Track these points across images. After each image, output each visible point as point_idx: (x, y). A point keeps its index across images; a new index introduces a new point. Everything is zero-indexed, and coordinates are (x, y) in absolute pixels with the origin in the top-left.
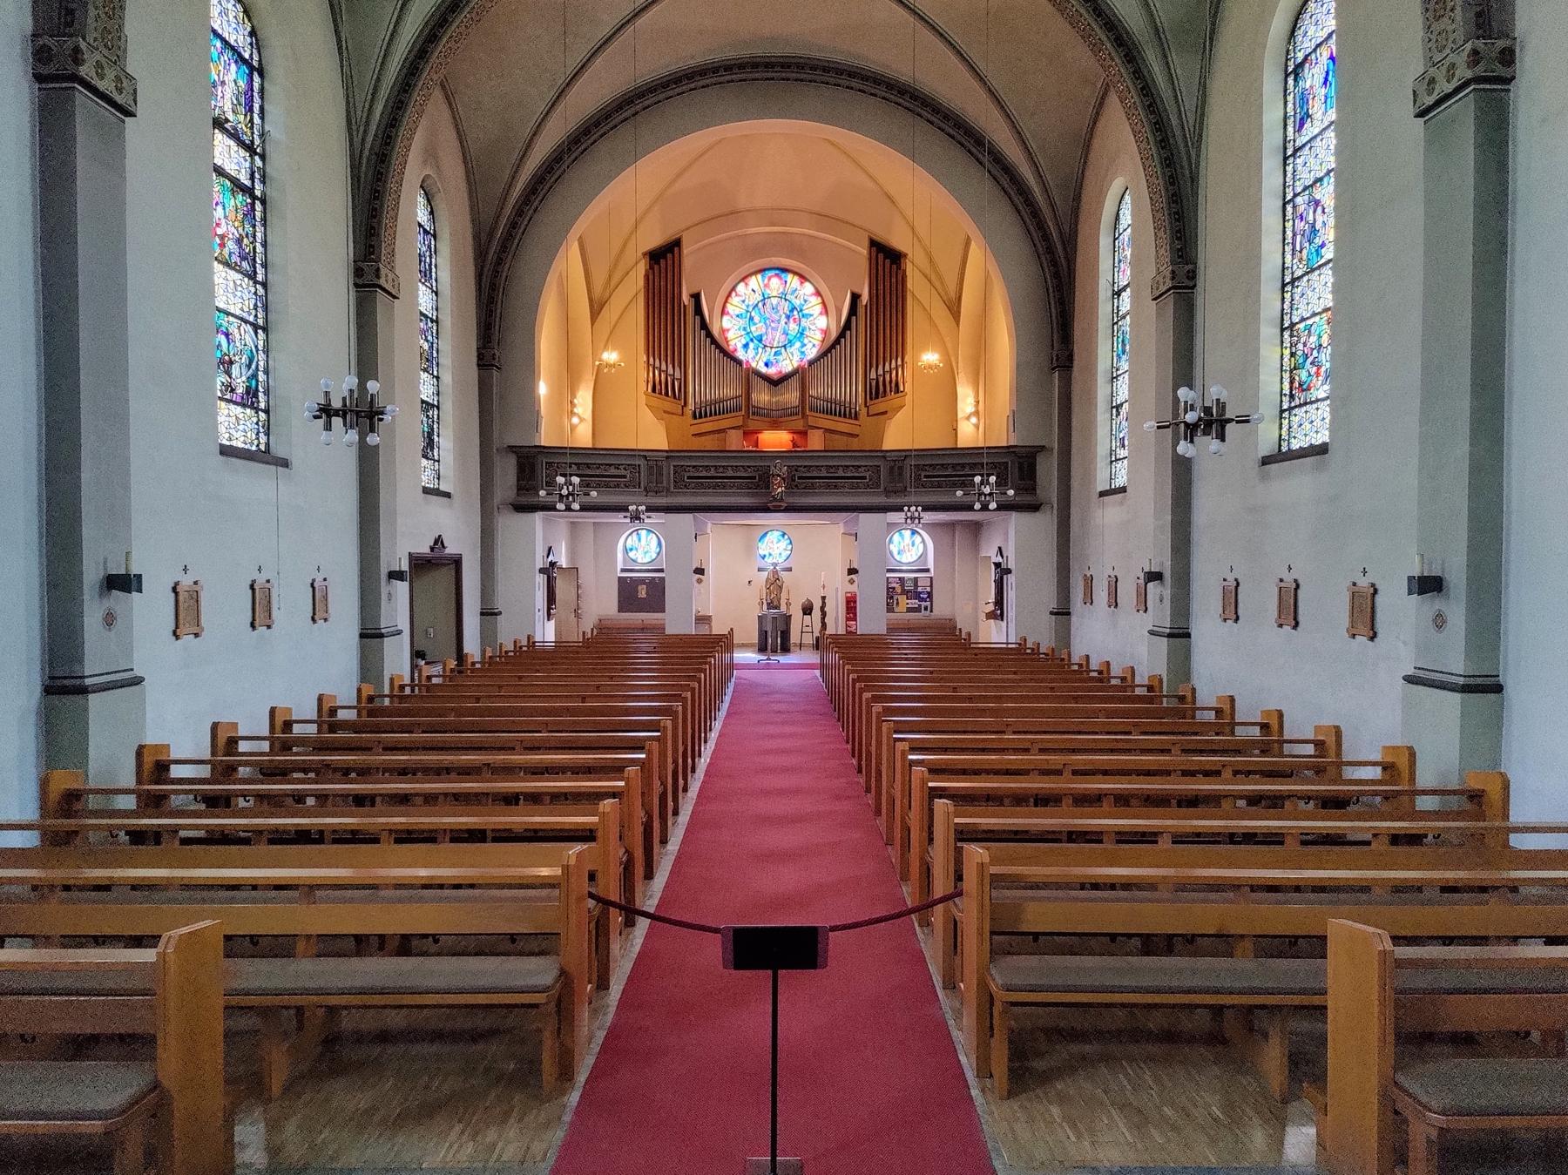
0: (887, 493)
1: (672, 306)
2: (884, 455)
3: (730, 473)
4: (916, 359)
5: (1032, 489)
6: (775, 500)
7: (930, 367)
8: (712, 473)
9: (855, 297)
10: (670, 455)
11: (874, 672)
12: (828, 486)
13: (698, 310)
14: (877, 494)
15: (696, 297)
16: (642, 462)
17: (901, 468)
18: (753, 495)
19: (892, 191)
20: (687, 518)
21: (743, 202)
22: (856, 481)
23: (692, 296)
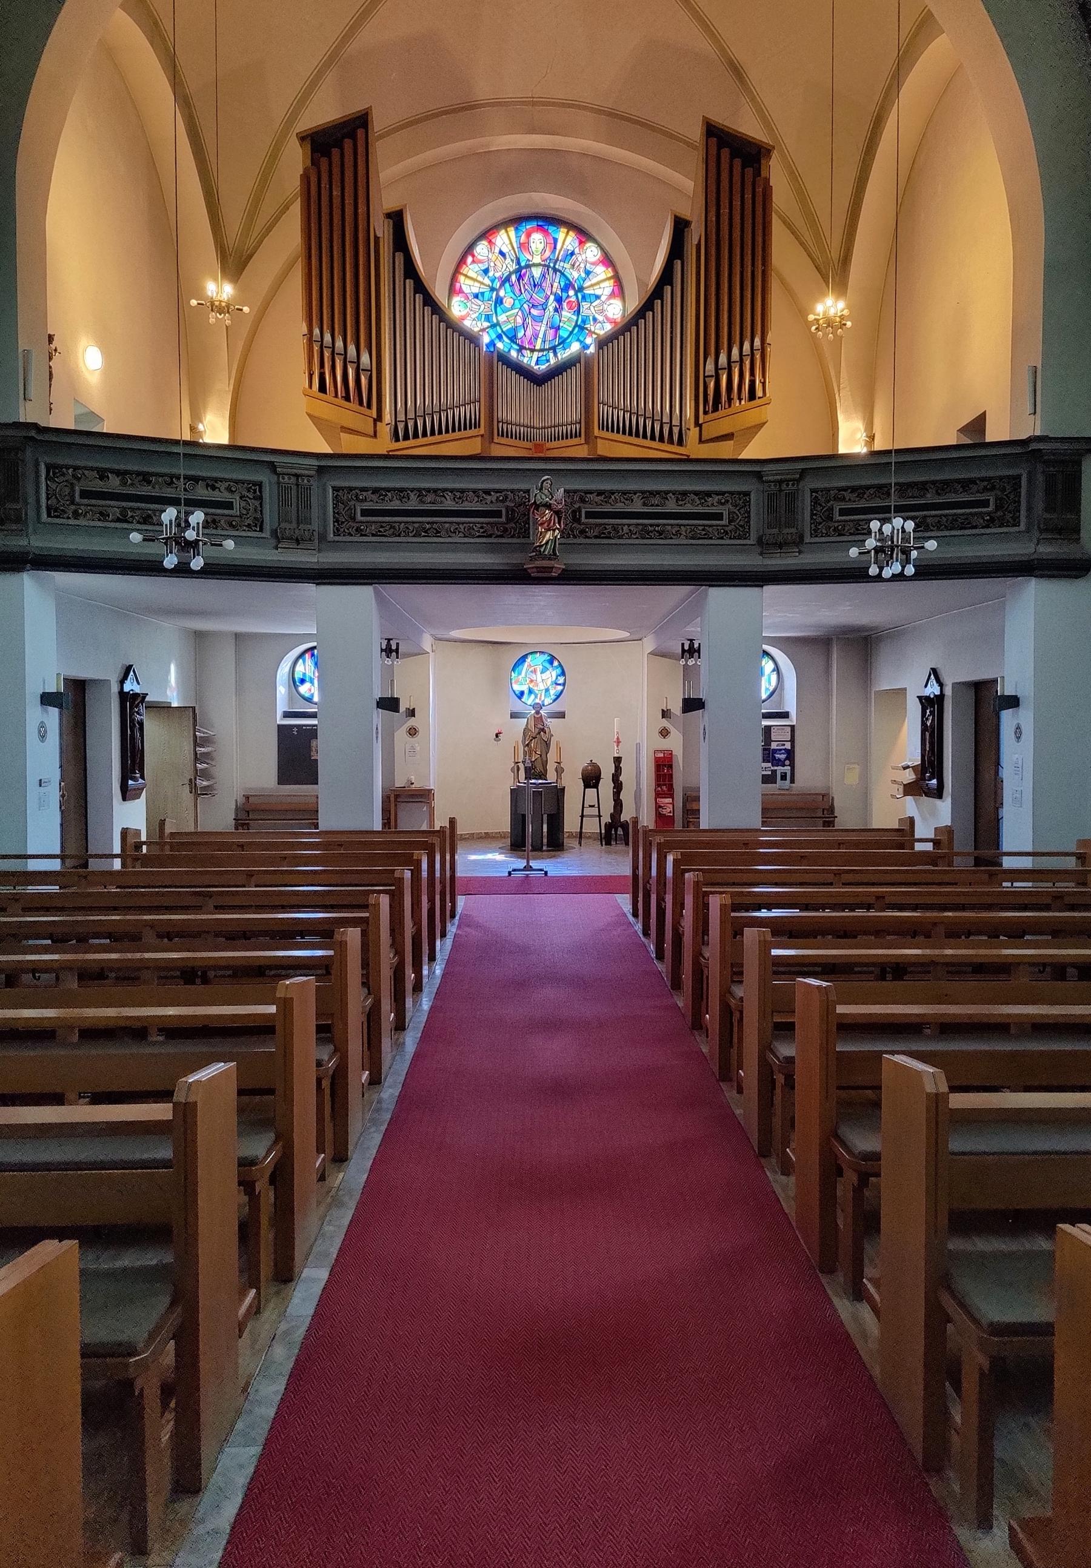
0: (765, 545)
1: (351, 245)
2: (756, 469)
3: (449, 504)
4: (801, 312)
5: (1071, 531)
6: (541, 556)
7: (829, 323)
8: (413, 504)
9: (680, 226)
10: (326, 466)
11: (741, 906)
12: (645, 533)
13: (400, 243)
14: (743, 549)
15: (397, 219)
16: (264, 476)
17: (792, 497)
18: (492, 549)
19: (740, 54)
20: (363, 595)
21: (483, 91)
22: (701, 524)
23: (389, 216)
